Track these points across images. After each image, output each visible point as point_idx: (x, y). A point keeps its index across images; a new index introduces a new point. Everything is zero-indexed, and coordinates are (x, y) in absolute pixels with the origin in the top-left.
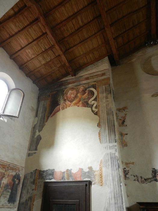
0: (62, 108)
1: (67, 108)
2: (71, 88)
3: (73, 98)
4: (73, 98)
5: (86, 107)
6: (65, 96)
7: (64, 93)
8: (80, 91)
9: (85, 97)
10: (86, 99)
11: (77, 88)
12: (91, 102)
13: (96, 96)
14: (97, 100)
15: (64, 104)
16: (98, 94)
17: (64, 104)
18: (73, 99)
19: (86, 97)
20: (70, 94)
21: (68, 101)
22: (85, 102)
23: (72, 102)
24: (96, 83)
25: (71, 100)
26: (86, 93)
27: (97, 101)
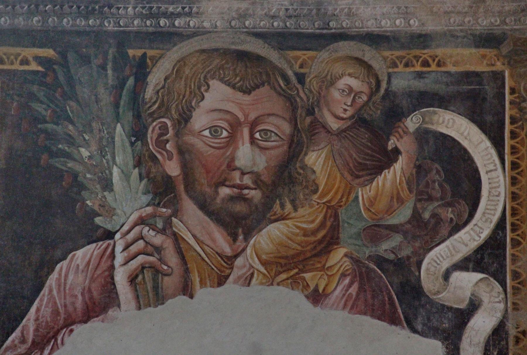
0: (132, 280)
1: (201, 293)
2: (225, 53)
3: (258, 183)
4: (258, 183)
5: (393, 321)
6: (161, 143)
7: (149, 93)
8: (334, 125)
9: (382, 204)
10: (394, 229)
11: (301, 78)
12: (447, 276)
13: (501, 225)
14: (503, 266)
15: (158, 240)
16: (514, 197)
17: (158, 240)
18: (255, 195)
19: (390, 211)
20: (214, 130)
21: (203, 206)
22: (380, 261)
23: (247, 236)
24: (499, 66)
25: (239, 208)
26: (398, 166)
27: (503, 284)
